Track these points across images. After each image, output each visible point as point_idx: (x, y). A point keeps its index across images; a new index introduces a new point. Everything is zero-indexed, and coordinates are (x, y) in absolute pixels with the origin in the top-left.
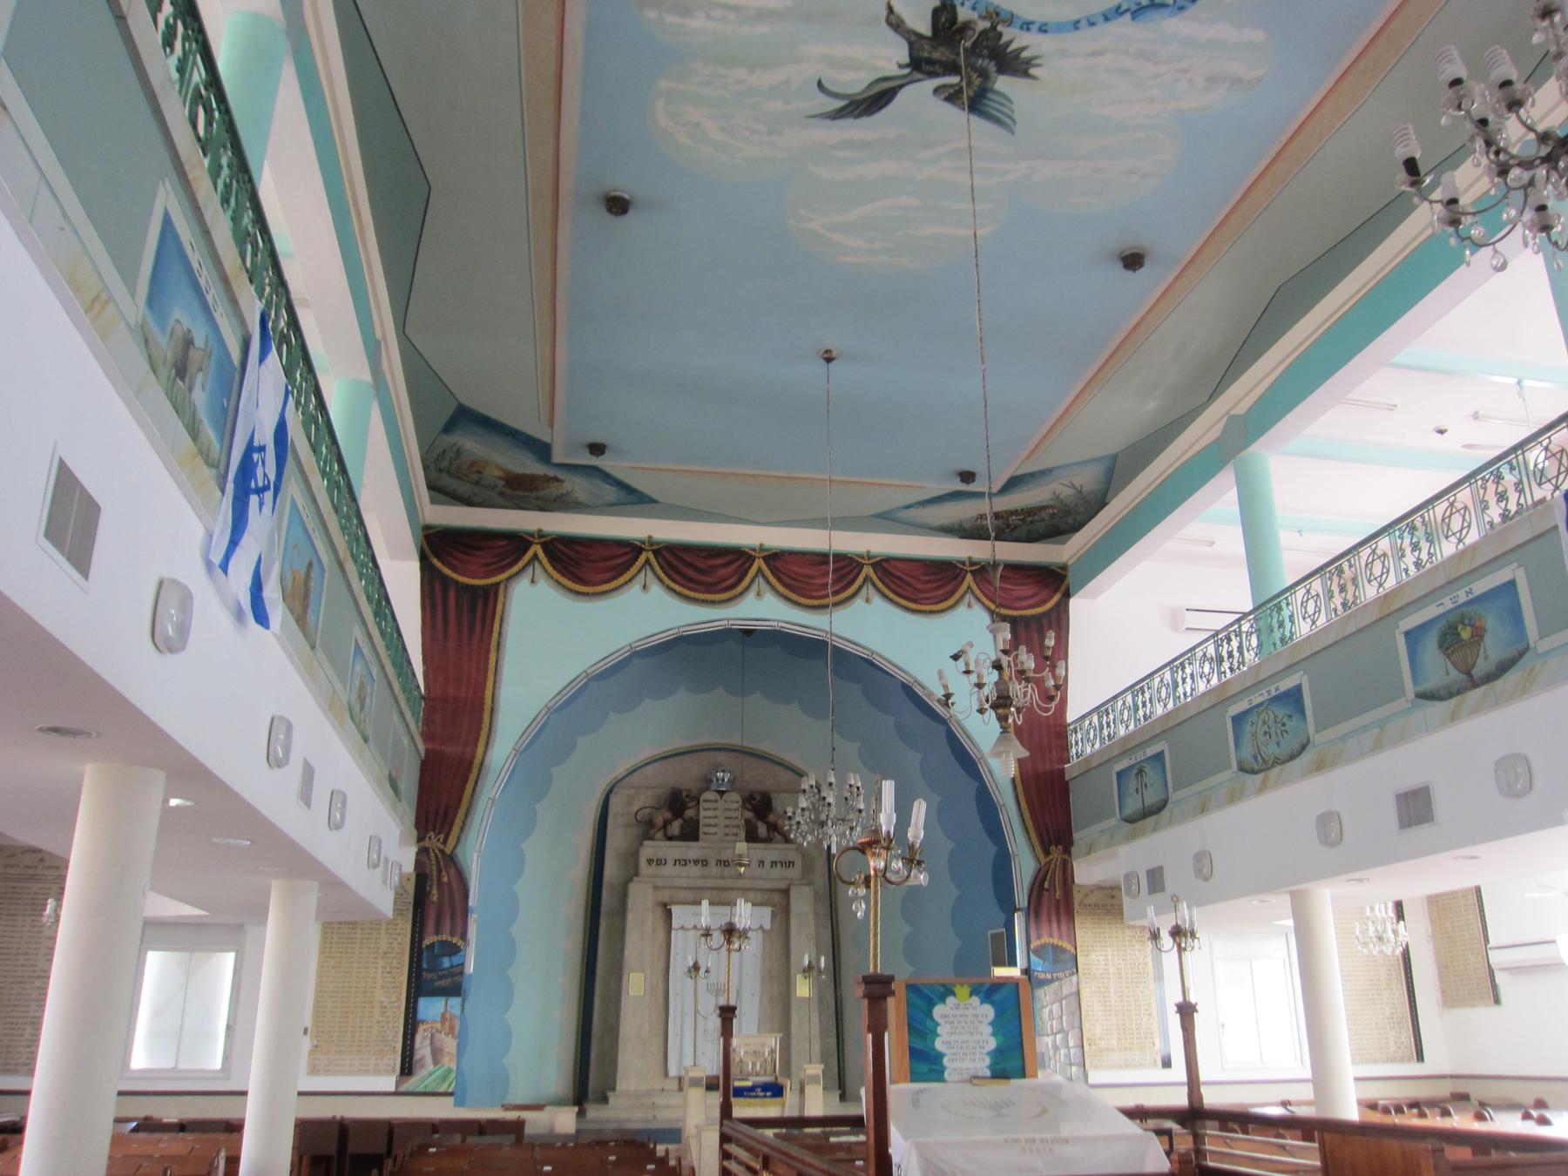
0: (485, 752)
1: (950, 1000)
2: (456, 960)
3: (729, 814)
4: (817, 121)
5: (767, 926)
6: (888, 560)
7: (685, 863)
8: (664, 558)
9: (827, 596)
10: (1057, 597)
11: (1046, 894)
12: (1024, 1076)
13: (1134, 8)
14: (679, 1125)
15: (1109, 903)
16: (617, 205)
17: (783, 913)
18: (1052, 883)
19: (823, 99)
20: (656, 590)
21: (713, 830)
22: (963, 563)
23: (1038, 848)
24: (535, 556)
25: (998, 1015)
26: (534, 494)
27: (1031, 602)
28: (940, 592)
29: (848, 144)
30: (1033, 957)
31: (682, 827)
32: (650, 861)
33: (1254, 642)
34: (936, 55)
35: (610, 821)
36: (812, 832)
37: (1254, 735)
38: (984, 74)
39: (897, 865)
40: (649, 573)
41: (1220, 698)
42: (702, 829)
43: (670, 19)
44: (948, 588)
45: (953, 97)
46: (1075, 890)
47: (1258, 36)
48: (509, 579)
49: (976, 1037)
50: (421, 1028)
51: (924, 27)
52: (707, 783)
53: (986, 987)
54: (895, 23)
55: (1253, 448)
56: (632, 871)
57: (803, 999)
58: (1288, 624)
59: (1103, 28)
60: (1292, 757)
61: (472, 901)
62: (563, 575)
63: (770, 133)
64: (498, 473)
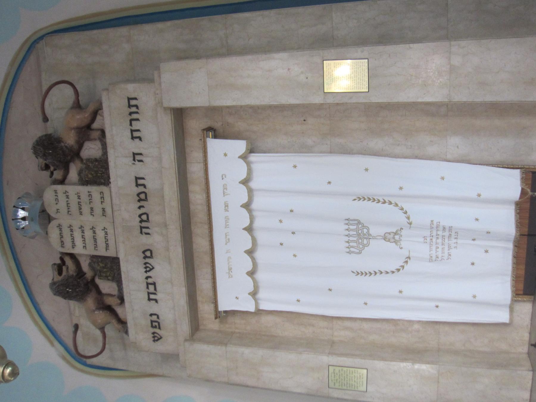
3: (74, 207)
5: (240, 146)
21: (100, 235)
31: (106, 278)
32: (156, 338)
42: (102, 252)
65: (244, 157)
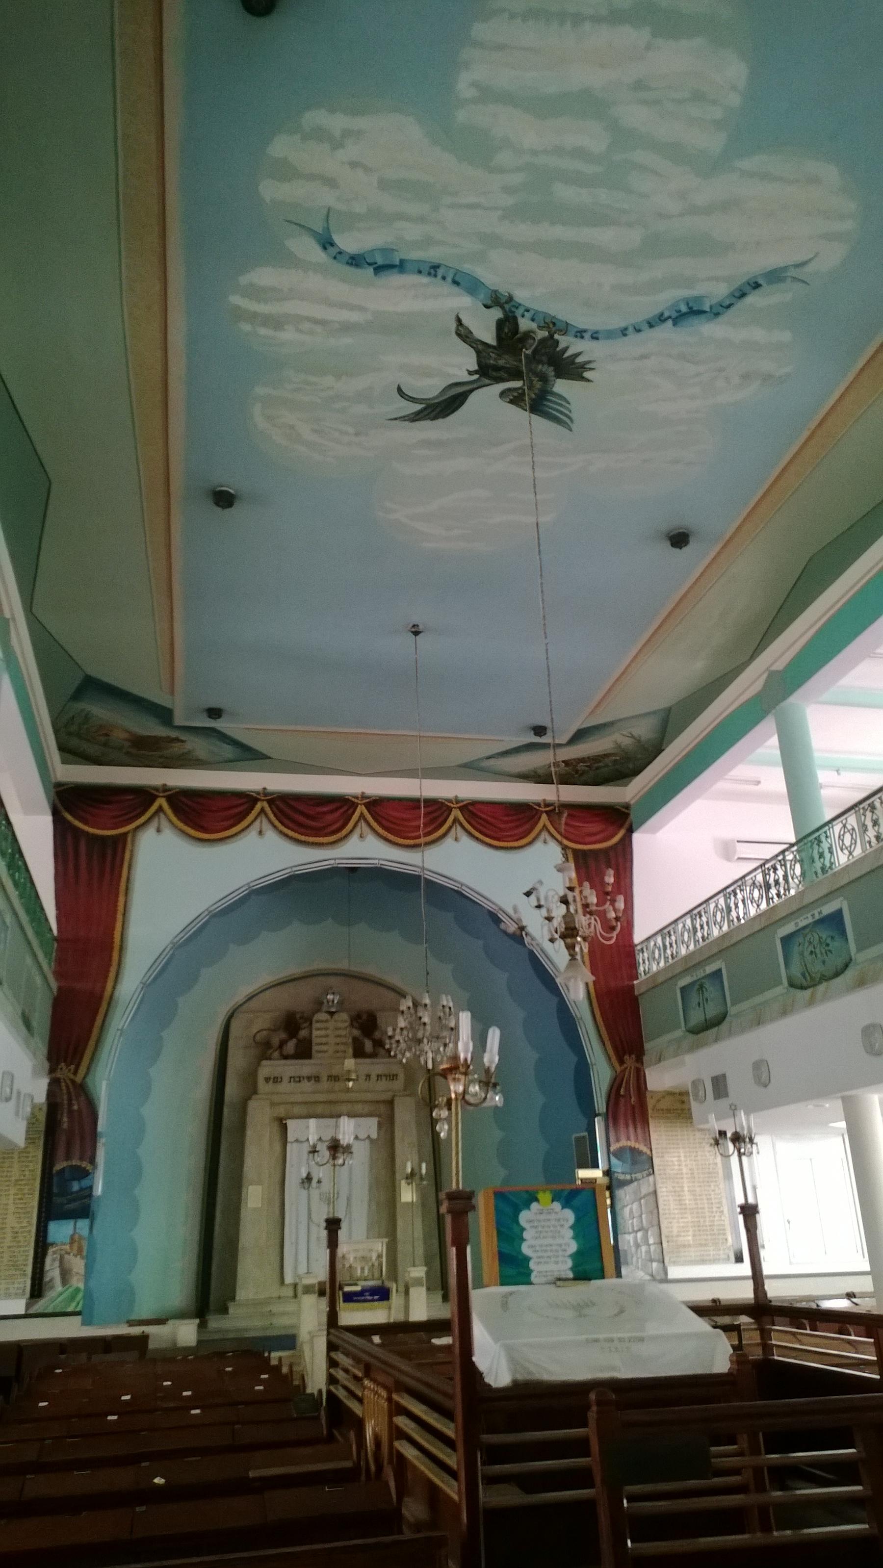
0: (114, 988)
1: (534, 1206)
2: (85, 1183)
4: (397, 422)
5: (374, 1136)
6: (474, 803)
7: (299, 1079)
8: (278, 808)
9: (419, 837)
10: (621, 833)
11: (622, 1100)
12: (603, 1277)
13: (674, 315)
14: (294, 1332)
15: (679, 1108)
16: (224, 499)
17: (388, 1123)
18: (627, 1089)
19: (404, 403)
20: (271, 836)
22: (539, 805)
23: (614, 1058)
24: (160, 809)
25: (578, 1220)
26: (158, 753)
27: (598, 837)
28: (521, 830)
29: (427, 444)
30: (614, 1160)
31: (297, 1046)
32: (267, 1080)
33: (798, 870)
34: (501, 362)
35: (231, 1043)
36: (410, 1049)
37: (802, 954)
38: (544, 379)
39: (475, 1088)
40: (265, 820)
41: (767, 923)
42: (315, 1048)
43: (263, 331)
44: (527, 826)
45: (515, 399)
46: (648, 1095)
47: (786, 336)
48: (138, 828)
49: (559, 1241)
50: (51, 1251)
51: (488, 336)
52: (319, 1004)
53: (566, 1193)
54: (464, 334)
55: (792, 699)
56: (251, 1090)
57: (407, 1203)
58: (827, 855)
59: (648, 333)
60: (837, 974)
61: (102, 1125)
62: (186, 824)
63: (357, 434)
64: (126, 736)
65: (369, 1137)
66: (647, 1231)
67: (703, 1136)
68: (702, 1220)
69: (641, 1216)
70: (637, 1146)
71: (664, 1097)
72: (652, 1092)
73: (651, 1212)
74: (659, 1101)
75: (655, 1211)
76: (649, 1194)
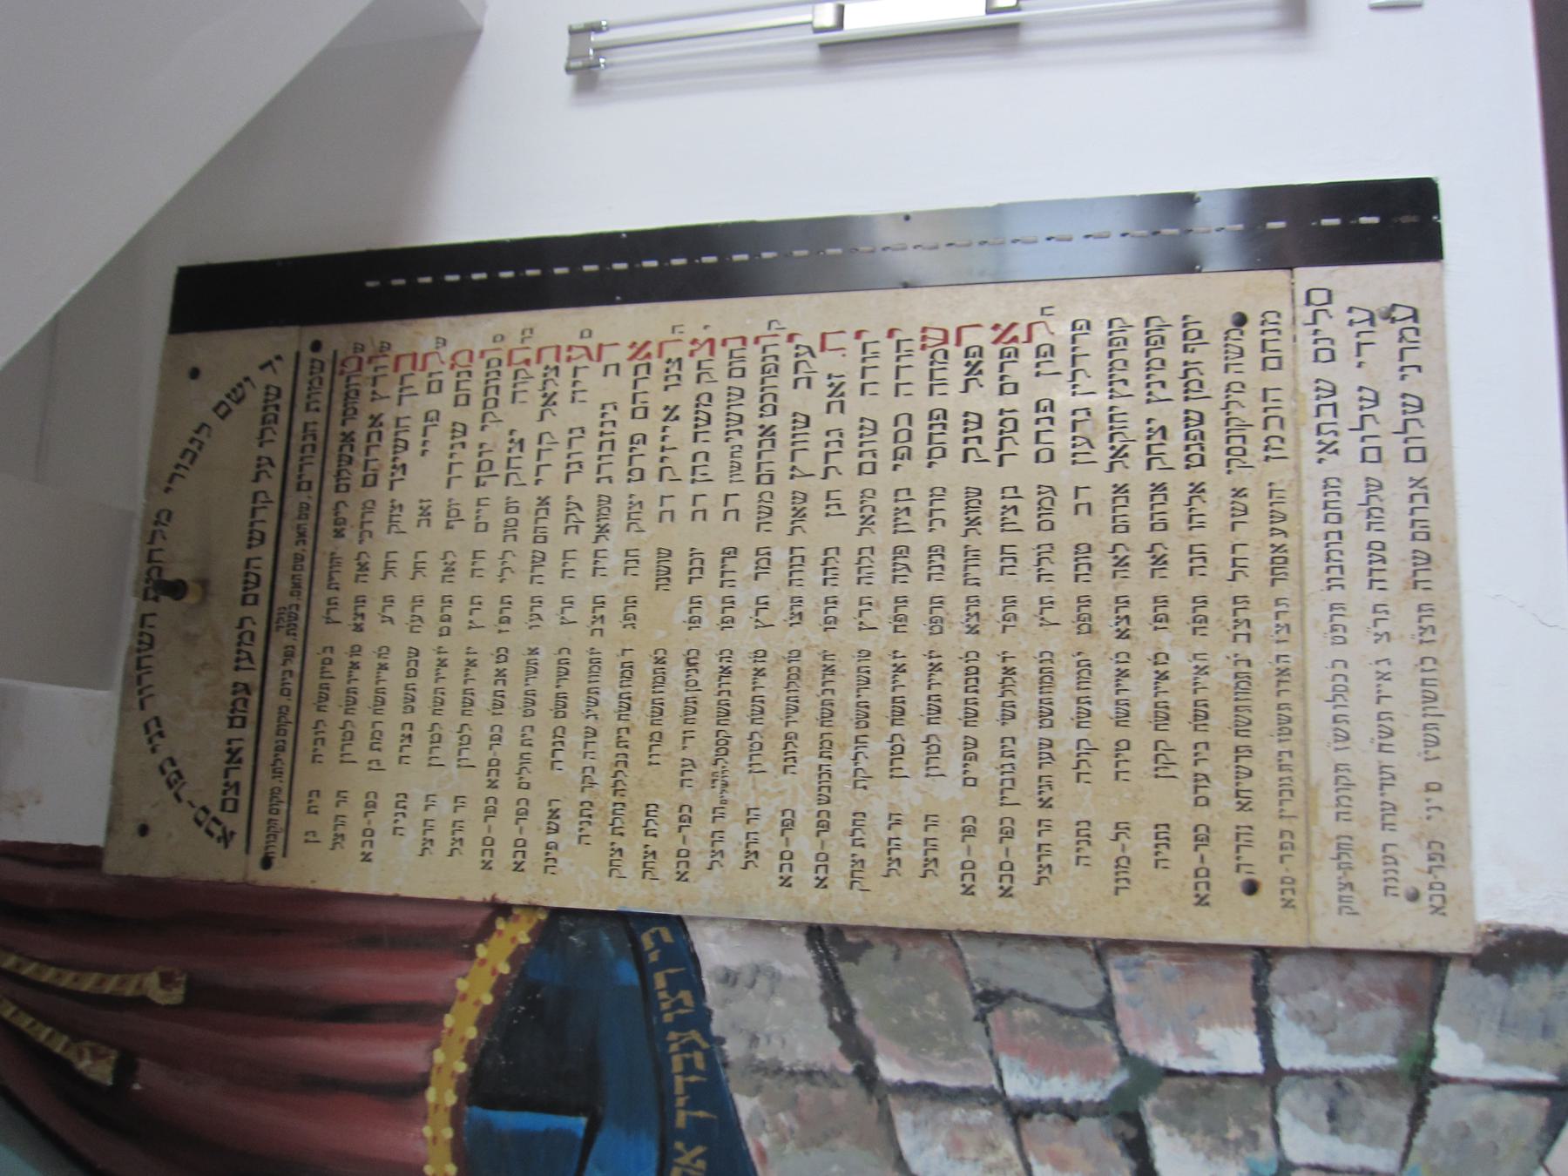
11: (151, 1078)
66: (1148, 1075)
67: (440, 437)
68: (1069, 529)
69: (1020, 1113)
70: (462, 1025)
71: (155, 730)
72: (110, 830)
73: (991, 998)
74: (175, 781)
75: (973, 955)
76: (835, 992)
